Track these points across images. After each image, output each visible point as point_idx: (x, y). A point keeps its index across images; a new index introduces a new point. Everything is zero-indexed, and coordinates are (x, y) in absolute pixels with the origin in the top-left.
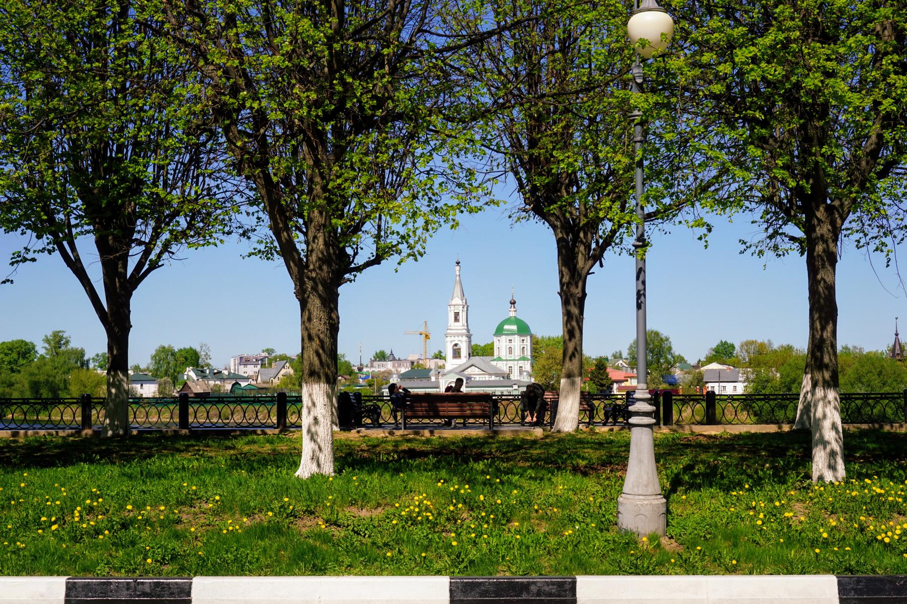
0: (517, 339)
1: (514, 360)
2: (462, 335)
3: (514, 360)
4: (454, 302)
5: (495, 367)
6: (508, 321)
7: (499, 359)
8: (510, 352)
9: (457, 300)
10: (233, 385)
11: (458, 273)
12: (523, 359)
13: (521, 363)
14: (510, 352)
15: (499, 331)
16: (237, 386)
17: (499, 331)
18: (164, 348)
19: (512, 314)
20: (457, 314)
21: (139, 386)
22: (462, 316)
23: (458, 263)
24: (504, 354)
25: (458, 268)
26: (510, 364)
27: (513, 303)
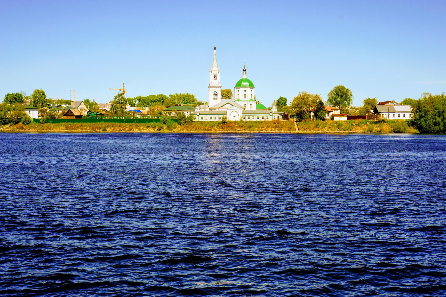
0: (248, 90)
1: (247, 101)
2: (218, 87)
3: (247, 101)
4: (213, 69)
5: (237, 104)
6: (242, 80)
7: (239, 100)
8: (245, 97)
9: (215, 68)
10: (88, 112)
11: (215, 53)
12: (251, 100)
13: (251, 103)
14: (245, 97)
15: (239, 85)
16: (90, 112)
17: (239, 85)
18: (38, 90)
19: (245, 77)
20: (215, 75)
21: (28, 112)
22: (218, 76)
23: (215, 48)
24: (242, 97)
25: (215, 51)
26: (245, 103)
27: (244, 71)
